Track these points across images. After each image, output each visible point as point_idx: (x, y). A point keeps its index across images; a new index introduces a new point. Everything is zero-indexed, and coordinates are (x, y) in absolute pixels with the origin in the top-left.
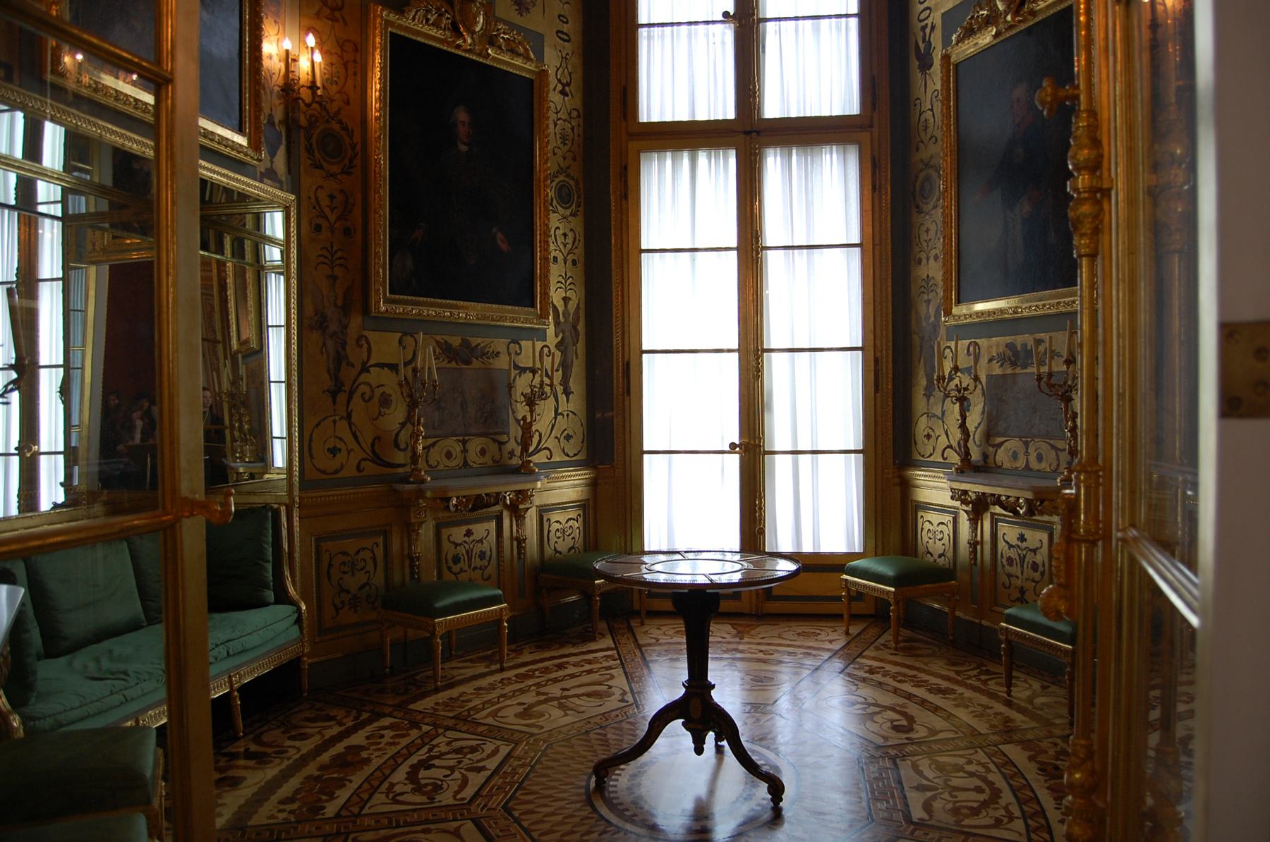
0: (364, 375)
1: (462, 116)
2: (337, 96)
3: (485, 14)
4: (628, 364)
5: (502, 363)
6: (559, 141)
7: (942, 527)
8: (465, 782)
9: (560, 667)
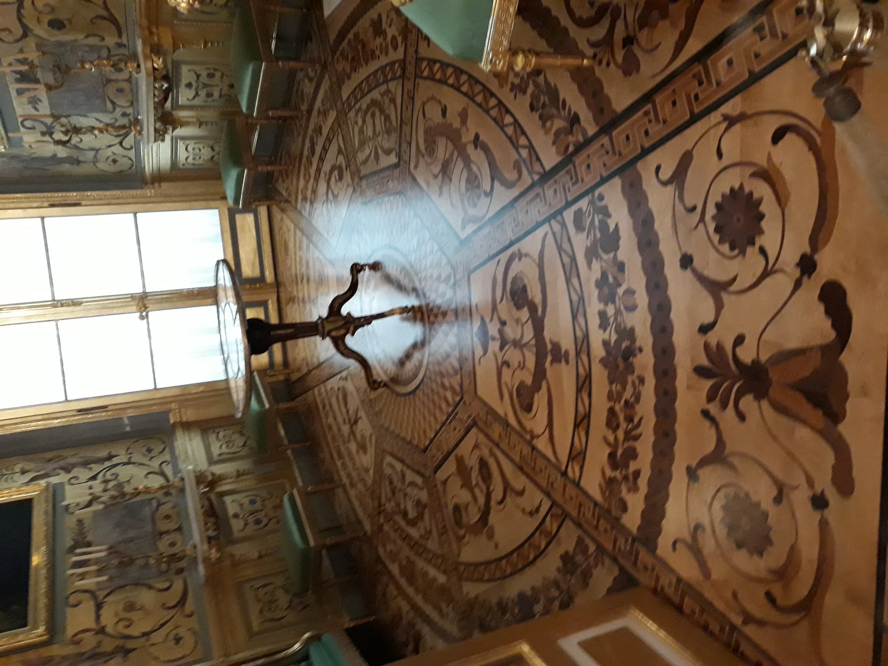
0: (109, 630)
4: (79, 411)
7: (190, 148)
8: (412, 484)
9: (330, 428)
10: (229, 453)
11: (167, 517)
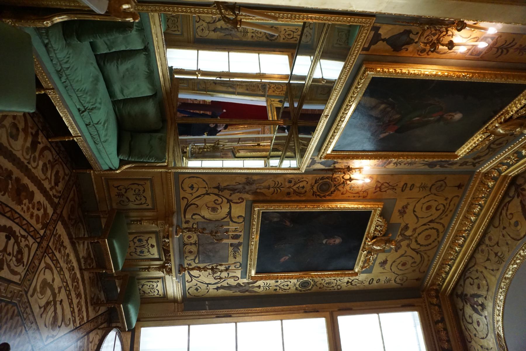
0: (226, 201)
1: (338, 241)
3: (380, 250)
4: (230, 316)
5: (231, 260)
6: (328, 281)
9: (78, 295)
11: (191, 252)
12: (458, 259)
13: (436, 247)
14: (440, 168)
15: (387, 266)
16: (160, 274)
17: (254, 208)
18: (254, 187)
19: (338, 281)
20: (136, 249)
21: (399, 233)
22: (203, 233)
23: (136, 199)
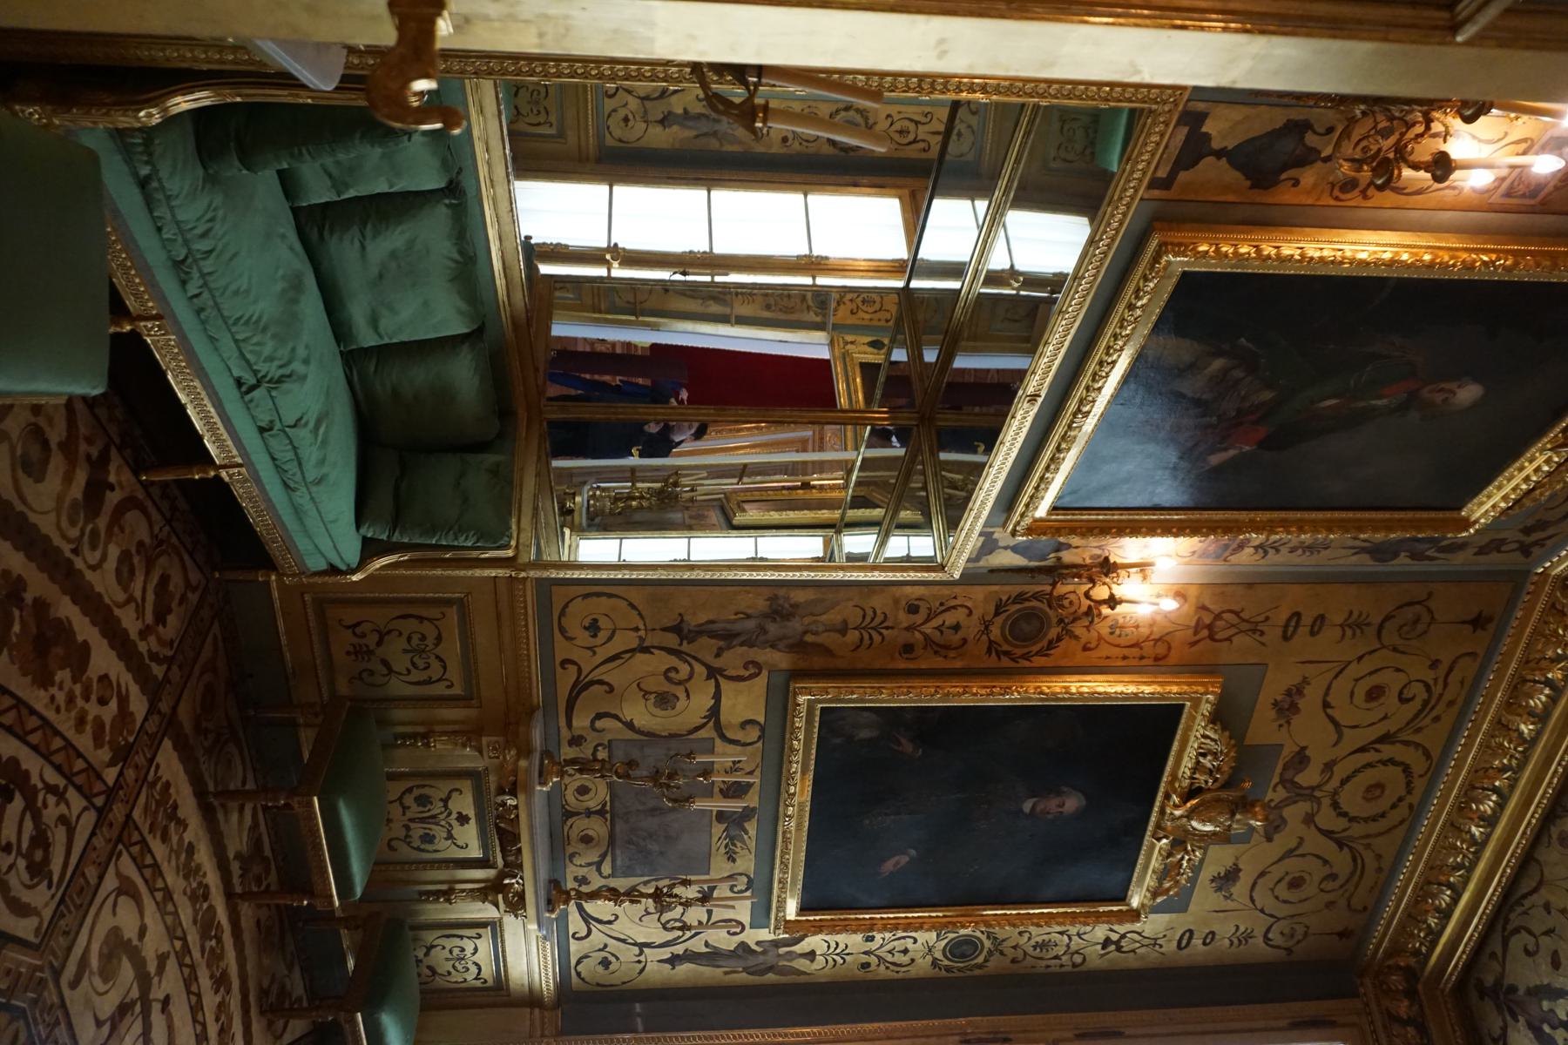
0: (704, 671)
1: (1072, 803)
2: (1094, 634)
3: (1214, 833)
5: (720, 867)
6: (1039, 939)
9: (221, 981)
10: (461, 937)
11: (586, 840)
12: (1481, 866)
13: (1405, 826)
14: (1408, 561)
15: (1240, 889)
16: (487, 911)
17: (795, 695)
18: (796, 625)
19: (1075, 938)
20: (408, 828)
21: (1276, 779)
22: (628, 776)
23: (413, 664)
